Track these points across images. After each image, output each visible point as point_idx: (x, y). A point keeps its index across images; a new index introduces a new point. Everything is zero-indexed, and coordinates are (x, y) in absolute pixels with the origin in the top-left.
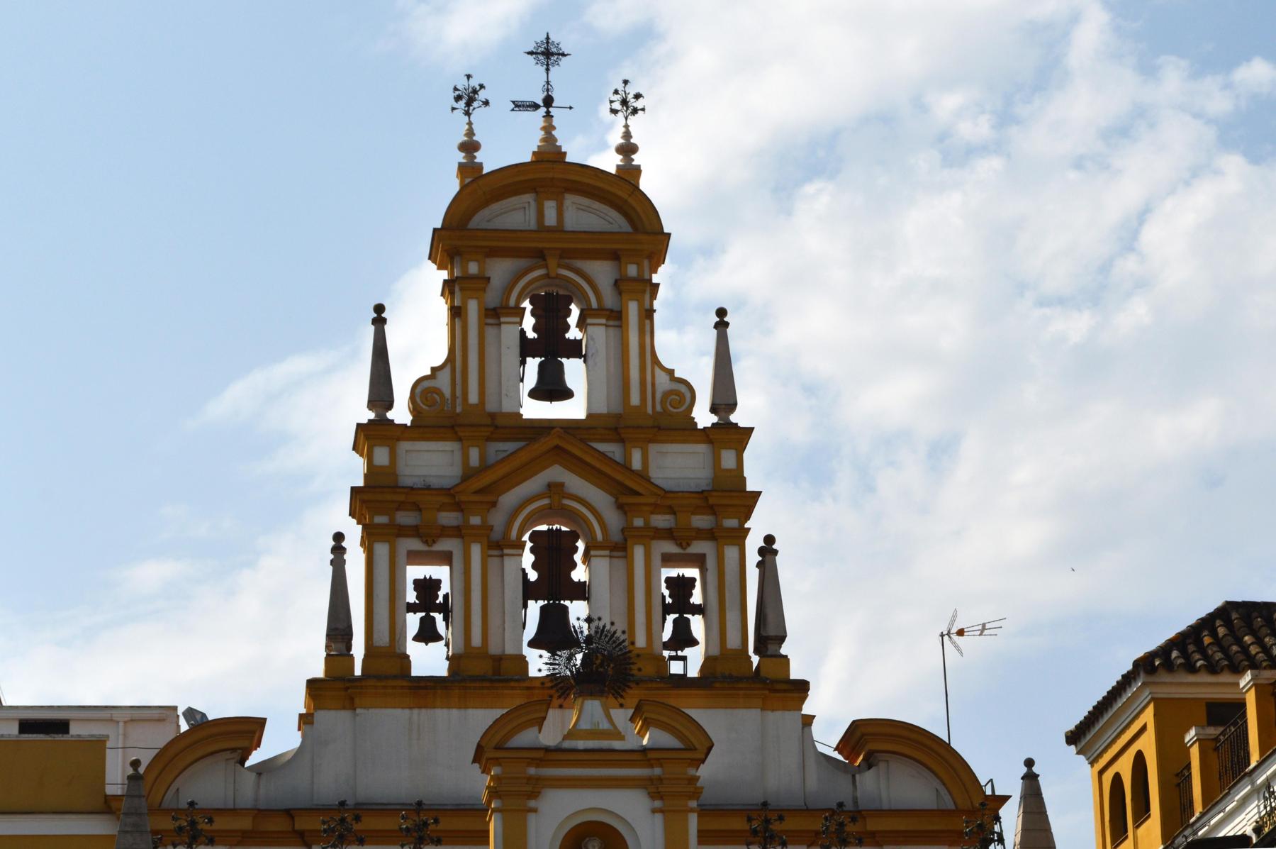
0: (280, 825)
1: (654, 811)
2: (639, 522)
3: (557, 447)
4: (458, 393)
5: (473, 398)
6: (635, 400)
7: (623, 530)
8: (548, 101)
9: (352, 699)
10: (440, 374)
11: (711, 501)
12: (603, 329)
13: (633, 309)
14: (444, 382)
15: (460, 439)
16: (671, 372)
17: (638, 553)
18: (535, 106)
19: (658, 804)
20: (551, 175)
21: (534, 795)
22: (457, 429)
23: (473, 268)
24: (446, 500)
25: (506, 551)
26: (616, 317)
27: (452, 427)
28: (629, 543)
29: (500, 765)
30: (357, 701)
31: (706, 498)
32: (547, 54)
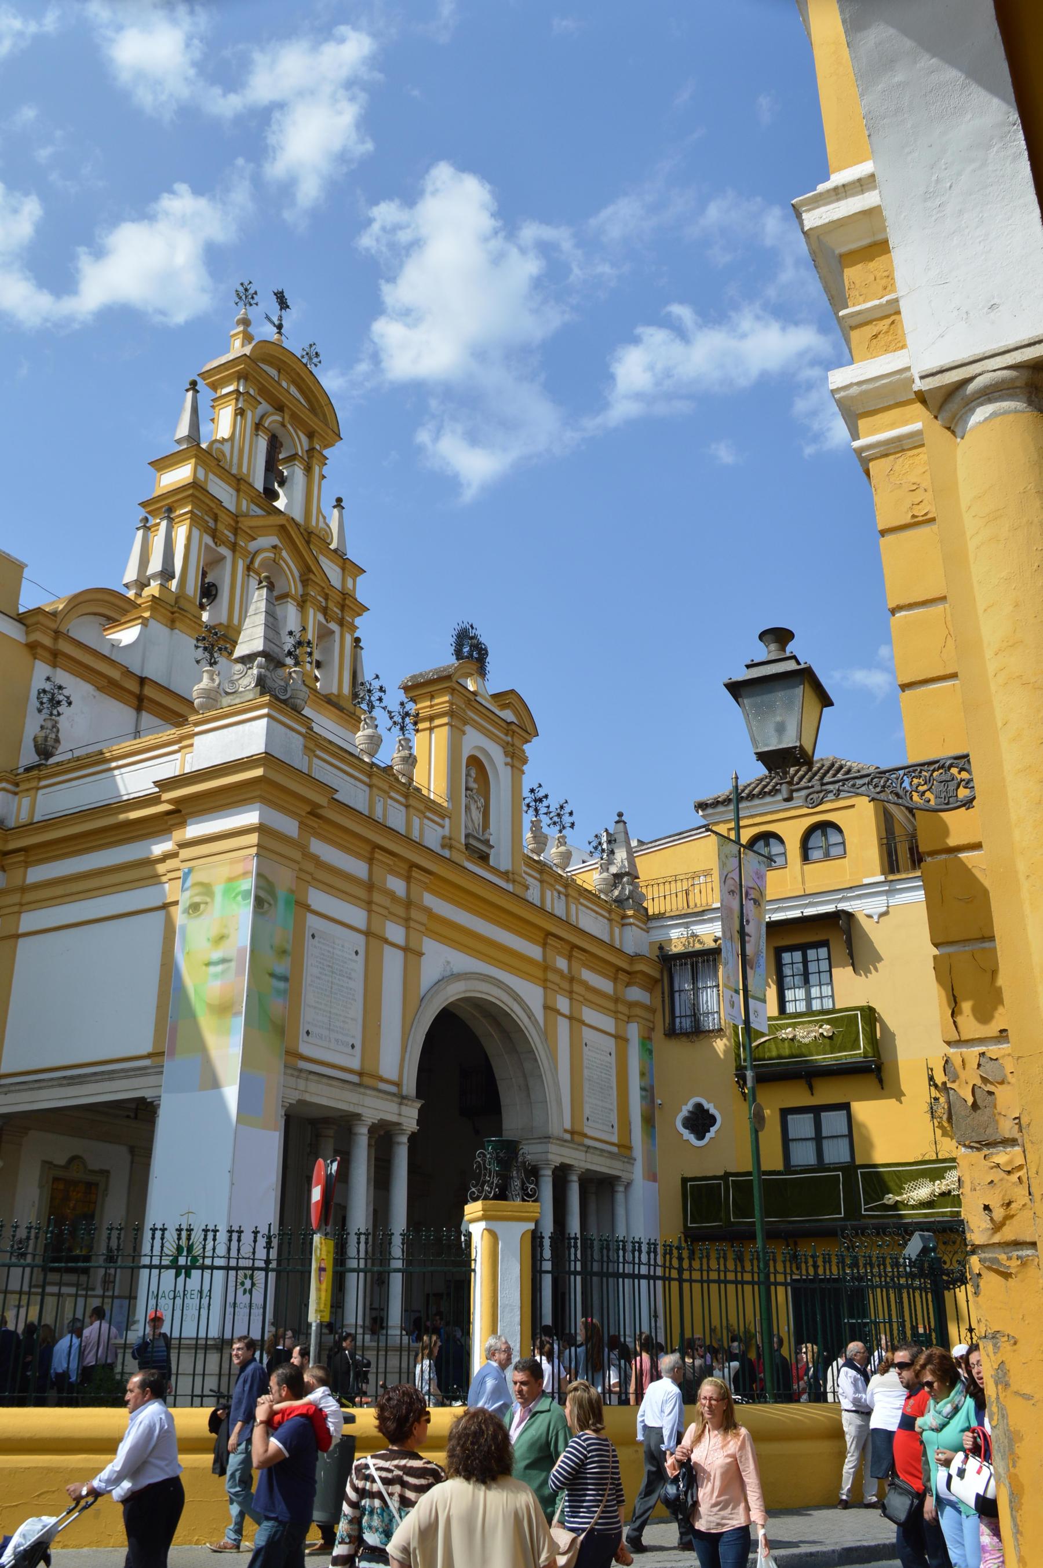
0: (133, 686)
1: (506, 764)
2: (312, 593)
3: (283, 527)
4: (235, 460)
5: (245, 470)
6: (314, 523)
7: (301, 596)
8: (280, 327)
9: (173, 621)
10: (225, 443)
11: (347, 602)
12: (302, 472)
13: (317, 469)
14: (226, 448)
15: (238, 491)
16: (324, 518)
17: (311, 612)
18: (274, 325)
19: (509, 760)
20: (295, 367)
21: (465, 723)
22: (242, 481)
23: (252, 392)
24: (232, 523)
25: (251, 573)
26: (308, 470)
27: (239, 480)
28: (308, 604)
29: (452, 694)
30: (178, 624)
31: (344, 599)
32: (282, 300)
